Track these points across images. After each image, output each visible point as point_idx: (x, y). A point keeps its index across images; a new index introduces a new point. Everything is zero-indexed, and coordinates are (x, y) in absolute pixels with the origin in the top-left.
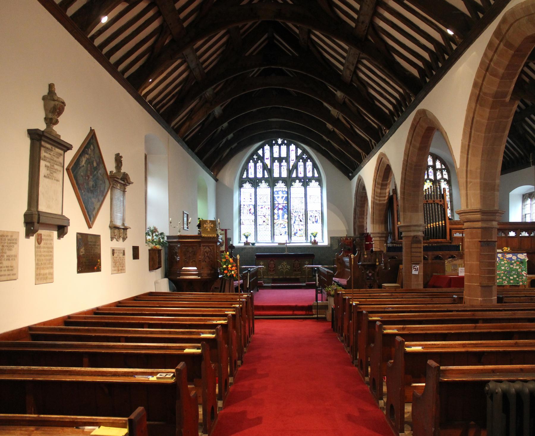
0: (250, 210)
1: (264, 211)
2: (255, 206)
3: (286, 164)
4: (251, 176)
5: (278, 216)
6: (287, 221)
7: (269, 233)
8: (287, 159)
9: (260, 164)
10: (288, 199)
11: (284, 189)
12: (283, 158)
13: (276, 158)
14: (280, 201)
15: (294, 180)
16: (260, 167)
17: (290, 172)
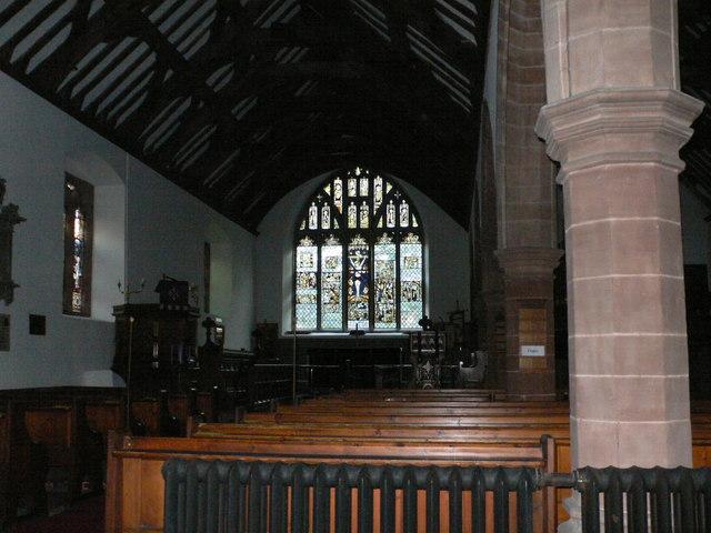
1: (333, 280)
2: (318, 274)
3: (367, 208)
4: (313, 227)
5: (355, 290)
8: (370, 199)
9: (326, 209)
10: (369, 263)
11: (363, 248)
12: (364, 198)
13: (352, 199)
14: (358, 267)
15: (380, 233)
17: (373, 220)
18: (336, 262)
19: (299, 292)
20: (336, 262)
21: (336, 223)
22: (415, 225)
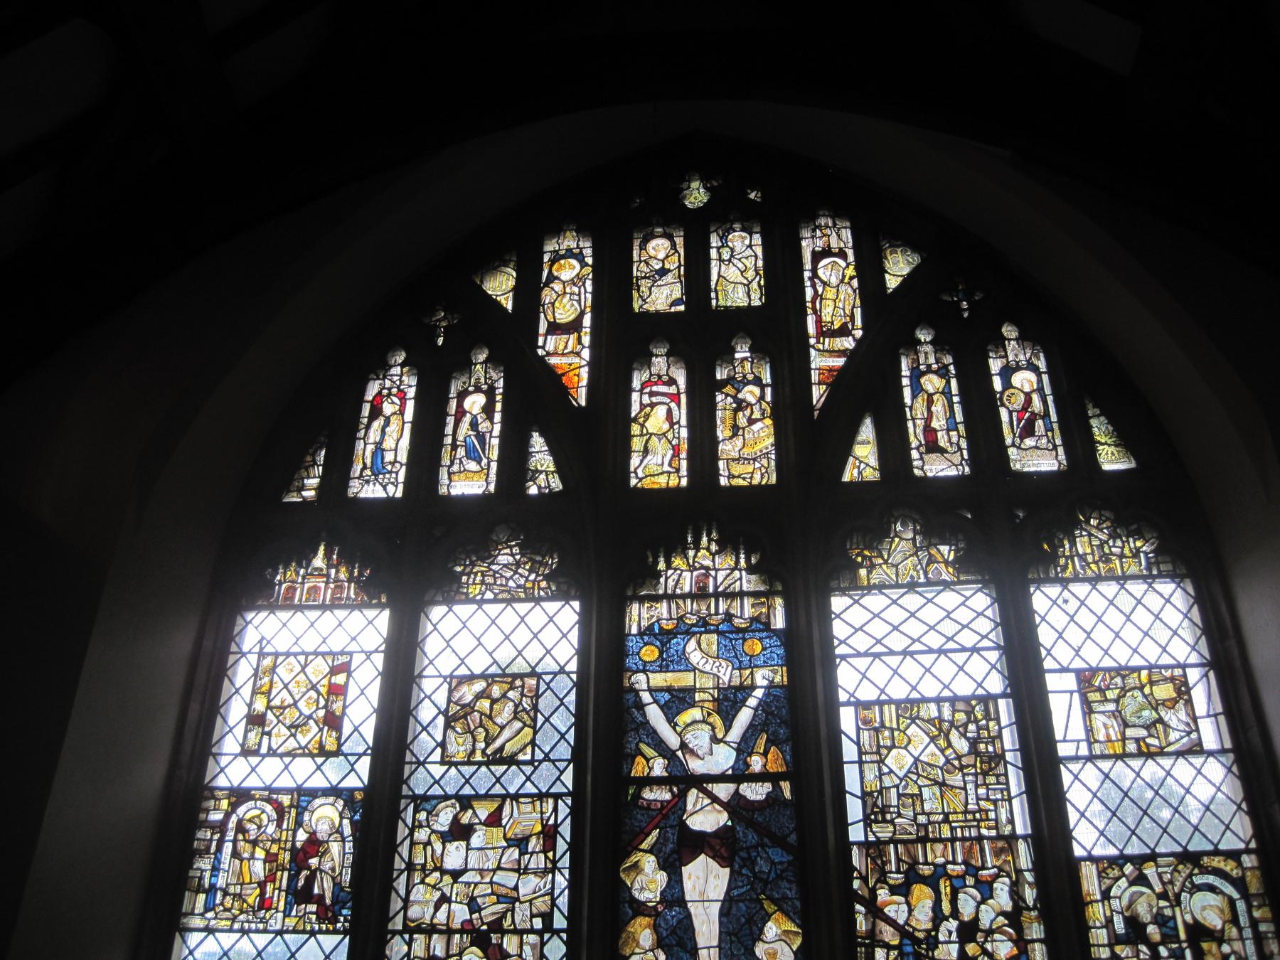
0: (300, 857)
8: (778, 325)
10: (801, 720)
12: (739, 320)
13: (658, 325)
16: (475, 403)
17: (810, 438)
18: (529, 716)
21: (540, 454)
22: (1112, 460)
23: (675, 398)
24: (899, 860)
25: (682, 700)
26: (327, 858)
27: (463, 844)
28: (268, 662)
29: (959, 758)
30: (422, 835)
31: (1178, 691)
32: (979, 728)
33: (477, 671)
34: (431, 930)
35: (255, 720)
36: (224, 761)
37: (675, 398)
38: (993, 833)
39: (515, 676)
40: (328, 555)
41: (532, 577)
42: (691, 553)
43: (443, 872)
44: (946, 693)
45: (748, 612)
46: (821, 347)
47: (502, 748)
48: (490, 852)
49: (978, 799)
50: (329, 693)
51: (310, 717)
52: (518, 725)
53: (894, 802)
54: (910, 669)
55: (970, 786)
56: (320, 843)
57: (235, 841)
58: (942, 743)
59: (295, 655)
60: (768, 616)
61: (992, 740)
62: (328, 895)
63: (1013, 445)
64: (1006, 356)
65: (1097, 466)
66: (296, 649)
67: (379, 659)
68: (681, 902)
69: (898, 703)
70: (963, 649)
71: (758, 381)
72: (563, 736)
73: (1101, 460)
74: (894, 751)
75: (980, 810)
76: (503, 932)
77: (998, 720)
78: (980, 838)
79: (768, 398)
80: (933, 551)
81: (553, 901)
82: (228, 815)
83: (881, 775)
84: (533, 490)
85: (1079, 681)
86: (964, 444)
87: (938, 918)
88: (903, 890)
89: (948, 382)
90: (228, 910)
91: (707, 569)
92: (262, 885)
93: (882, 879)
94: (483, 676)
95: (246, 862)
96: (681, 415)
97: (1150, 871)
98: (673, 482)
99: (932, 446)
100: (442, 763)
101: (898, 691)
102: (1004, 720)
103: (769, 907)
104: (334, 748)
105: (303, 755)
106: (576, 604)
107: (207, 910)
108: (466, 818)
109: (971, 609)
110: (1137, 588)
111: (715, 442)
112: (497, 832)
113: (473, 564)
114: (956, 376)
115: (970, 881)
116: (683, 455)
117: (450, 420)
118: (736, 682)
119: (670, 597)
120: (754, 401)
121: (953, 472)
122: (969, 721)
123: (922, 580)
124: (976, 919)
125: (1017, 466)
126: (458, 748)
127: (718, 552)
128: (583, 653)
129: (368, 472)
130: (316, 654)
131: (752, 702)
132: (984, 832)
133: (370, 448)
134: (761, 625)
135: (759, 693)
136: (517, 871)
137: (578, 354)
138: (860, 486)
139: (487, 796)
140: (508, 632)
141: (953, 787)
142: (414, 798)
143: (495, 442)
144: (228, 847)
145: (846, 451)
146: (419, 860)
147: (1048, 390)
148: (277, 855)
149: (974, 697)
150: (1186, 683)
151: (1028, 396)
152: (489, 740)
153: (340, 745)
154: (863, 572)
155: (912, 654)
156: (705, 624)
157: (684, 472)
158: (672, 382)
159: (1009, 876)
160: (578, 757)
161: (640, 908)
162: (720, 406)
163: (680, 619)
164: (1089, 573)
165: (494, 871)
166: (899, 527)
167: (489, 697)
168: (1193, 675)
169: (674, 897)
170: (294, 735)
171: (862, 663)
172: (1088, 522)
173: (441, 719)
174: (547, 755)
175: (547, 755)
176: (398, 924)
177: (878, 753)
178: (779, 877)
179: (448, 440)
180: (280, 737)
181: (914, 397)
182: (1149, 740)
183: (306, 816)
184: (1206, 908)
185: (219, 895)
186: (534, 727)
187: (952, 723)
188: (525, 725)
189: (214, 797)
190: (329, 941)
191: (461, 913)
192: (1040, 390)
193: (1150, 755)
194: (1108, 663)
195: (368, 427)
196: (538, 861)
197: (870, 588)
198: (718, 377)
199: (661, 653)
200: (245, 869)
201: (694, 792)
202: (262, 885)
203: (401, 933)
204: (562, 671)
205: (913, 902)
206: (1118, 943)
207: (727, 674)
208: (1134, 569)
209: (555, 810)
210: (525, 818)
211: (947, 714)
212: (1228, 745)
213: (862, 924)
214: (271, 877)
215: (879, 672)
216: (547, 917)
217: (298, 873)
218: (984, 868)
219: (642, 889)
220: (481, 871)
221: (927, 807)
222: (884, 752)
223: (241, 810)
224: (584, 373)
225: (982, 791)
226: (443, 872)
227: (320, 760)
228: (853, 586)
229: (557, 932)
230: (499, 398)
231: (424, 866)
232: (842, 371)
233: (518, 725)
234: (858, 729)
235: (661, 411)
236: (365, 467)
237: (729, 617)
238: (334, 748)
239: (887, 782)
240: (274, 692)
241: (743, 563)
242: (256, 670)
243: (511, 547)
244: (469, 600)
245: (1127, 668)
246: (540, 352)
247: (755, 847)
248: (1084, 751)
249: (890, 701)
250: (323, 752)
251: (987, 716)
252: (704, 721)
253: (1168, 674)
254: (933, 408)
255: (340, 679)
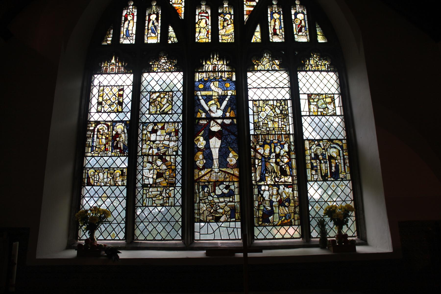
1: (161, 139)
5: (208, 156)
6: (237, 173)
7: (177, 213)
16: (153, 17)
17: (243, 30)
18: (171, 102)
19: (91, 161)
20: (171, 102)
21: (171, 32)
22: (321, 39)
23: (208, 17)
24: (262, 139)
25: (209, 98)
26: (121, 138)
27: (155, 134)
28: (102, 88)
29: (277, 114)
30: (145, 132)
31: (332, 100)
32: (283, 107)
33: (157, 90)
34: (148, 155)
35: (100, 103)
36: (92, 114)
37: (208, 17)
38: (285, 133)
39: (167, 92)
40: (115, 60)
41: (170, 66)
42: (212, 60)
43: (151, 141)
44: (275, 98)
45: (226, 76)
46: (247, 4)
47: (164, 110)
48: (162, 136)
49: (282, 125)
50: (118, 96)
51: (114, 102)
52: (168, 104)
53: (261, 125)
54: (267, 92)
55: (280, 122)
56: (119, 134)
57: (97, 134)
58: (273, 110)
59: (109, 86)
60: (231, 77)
61: (286, 110)
62: (122, 147)
63: (296, 34)
64: (296, 9)
65: (317, 41)
66: (109, 85)
67: (131, 87)
68: (209, 148)
69: (263, 100)
70: (280, 87)
71: (230, 13)
72: (179, 107)
73: (318, 39)
74: (262, 112)
75: (282, 127)
76: (166, 155)
77: (287, 105)
78: (282, 134)
79: (233, 18)
80: (274, 62)
81: (178, 148)
82: (95, 128)
83: (258, 118)
84: (170, 42)
85: (308, 97)
86: (283, 33)
87: (271, 153)
88: (263, 146)
89: (280, 16)
90: (96, 151)
91: (216, 64)
92: (105, 145)
93: (258, 143)
94: (158, 92)
95: (100, 140)
96: (209, 22)
97: (321, 143)
98: (207, 41)
99: (275, 34)
100: (149, 114)
101: (263, 97)
102: (289, 105)
103: (230, 149)
104: (121, 110)
105: (113, 112)
106: (182, 73)
107: (92, 151)
108: (156, 128)
109: (282, 77)
110: (324, 74)
111: (218, 30)
112: (164, 131)
113: (155, 62)
114: (283, 14)
115: (279, 144)
116: (210, 33)
117: (147, 22)
118: (223, 94)
119: (206, 72)
120: (229, 19)
121: (280, 41)
122: (280, 105)
123: (271, 69)
124: (280, 153)
125: (296, 40)
126: (153, 110)
127: (219, 60)
128: (184, 86)
129: (125, 36)
130: (114, 86)
131: (227, 99)
132: (283, 133)
133: (125, 29)
134: (229, 79)
135: (229, 97)
136: (169, 141)
137: (181, 4)
138: (256, 43)
139: (161, 122)
140: (164, 79)
141: (276, 122)
142: (142, 123)
143: (159, 28)
144: (95, 136)
145: (253, 34)
146: (144, 138)
147: (306, 19)
148: (108, 138)
149: (282, 100)
150: (334, 98)
151: (301, 21)
152: (161, 108)
153: (122, 110)
154: (256, 66)
155: (267, 88)
156: (215, 79)
157: (210, 38)
158: (207, 13)
159: (288, 143)
160: (183, 112)
161: (199, 150)
162: (220, 20)
163: (209, 77)
164: (313, 69)
165: (163, 141)
166: (265, 55)
167: (160, 97)
168: (336, 96)
169: (208, 147)
170: (110, 107)
171: (255, 90)
172: (313, 56)
173: (148, 103)
174: (175, 112)
175: (175, 112)
176: (140, 154)
177: (258, 113)
178: (233, 142)
179: (146, 28)
180: (106, 108)
181: (271, 20)
182: (324, 112)
183: (115, 128)
184: (333, 152)
185: (94, 148)
186: (172, 105)
187: (276, 106)
188: (170, 104)
189: (90, 123)
190: (123, 158)
191: (155, 151)
192: (304, 19)
193: (324, 116)
194: (315, 92)
195: (124, 23)
196: (174, 138)
197: (257, 71)
198: (219, 11)
199: (204, 86)
200: (100, 141)
201: (212, 121)
202: (105, 145)
203: (141, 156)
204: (179, 91)
205: (265, 149)
206: (312, 159)
207: (220, 92)
208: (324, 69)
209: (178, 126)
210: (170, 128)
211: (275, 104)
212: (342, 114)
213: (252, 154)
214: (107, 143)
215: (259, 92)
216: (177, 152)
217: (114, 142)
218: (282, 141)
219: (200, 145)
220: (160, 141)
221: (269, 126)
222: (259, 112)
223: (98, 127)
224: (183, 9)
225: (283, 123)
226: (151, 141)
227: (117, 114)
228: (253, 70)
229: (179, 155)
230: (160, 16)
231: (146, 140)
232: (252, 11)
233: (168, 104)
234: (253, 107)
235: (204, 21)
236: (124, 35)
237: (221, 77)
238: (121, 110)
239: (260, 120)
240: (104, 96)
241: (225, 63)
242: (99, 90)
243: (164, 58)
244: (154, 72)
245: (320, 94)
246: (171, 3)
247: (227, 135)
248: (308, 114)
249: (261, 100)
250: (118, 111)
251: (285, 105)
252: (215, 104)
253: (330, 96)
254: (276, 23)
255: (121, 93)
